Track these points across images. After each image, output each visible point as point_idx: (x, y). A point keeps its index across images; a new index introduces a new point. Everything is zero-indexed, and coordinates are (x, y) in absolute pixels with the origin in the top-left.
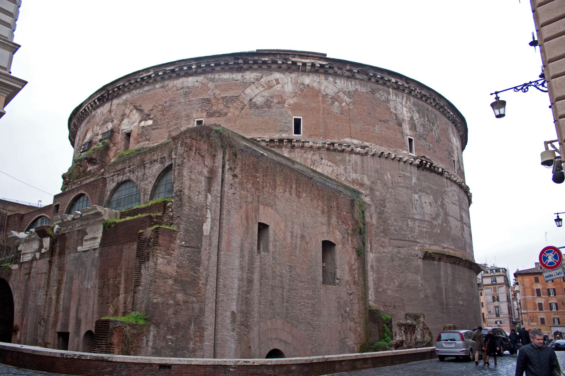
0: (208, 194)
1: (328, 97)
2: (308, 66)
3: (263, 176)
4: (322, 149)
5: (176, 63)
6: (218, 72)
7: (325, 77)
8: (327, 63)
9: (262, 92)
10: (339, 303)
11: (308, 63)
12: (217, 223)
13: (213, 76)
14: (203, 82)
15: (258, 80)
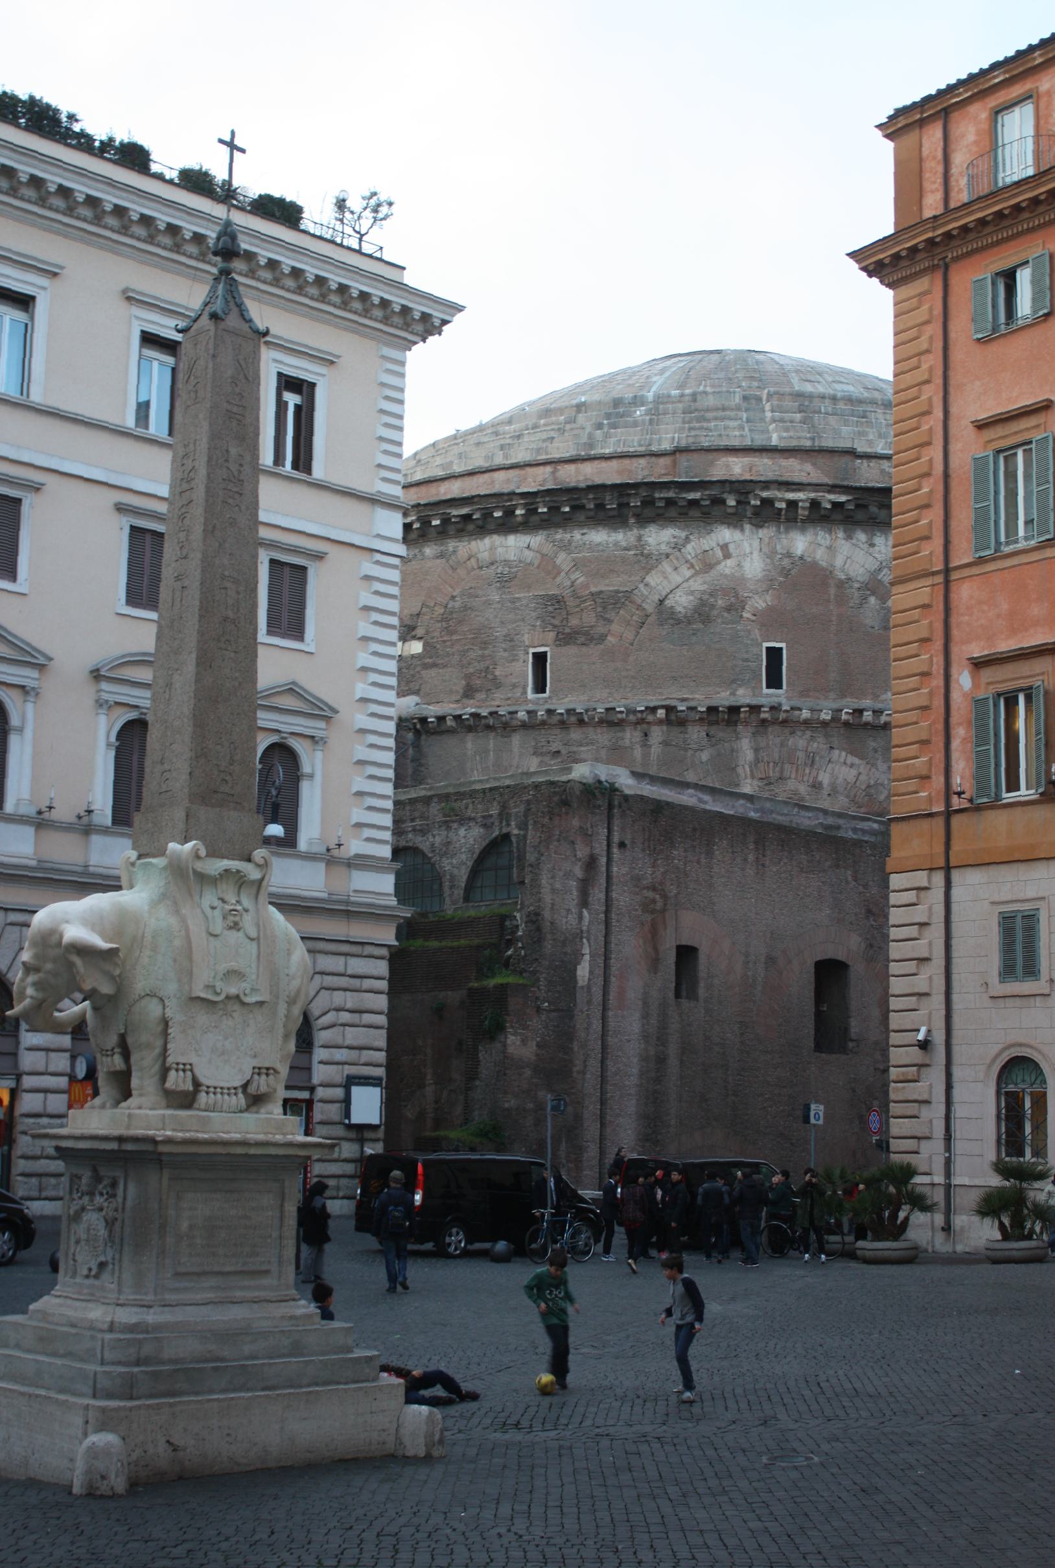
0: (584, 910)
1: (851, 587)
2: (803, 508)
3: (686, 851)
4: (833, 725)
5: (476, 500)
6: (581, 525)
7: (845, 531)
8: (850, 498)
9: (687, 580)
10: (854, 1091)
11: (801, 501)
12: (601, 961)
13: (568, 536)
14: (545, 551)
15: (677, 547)
